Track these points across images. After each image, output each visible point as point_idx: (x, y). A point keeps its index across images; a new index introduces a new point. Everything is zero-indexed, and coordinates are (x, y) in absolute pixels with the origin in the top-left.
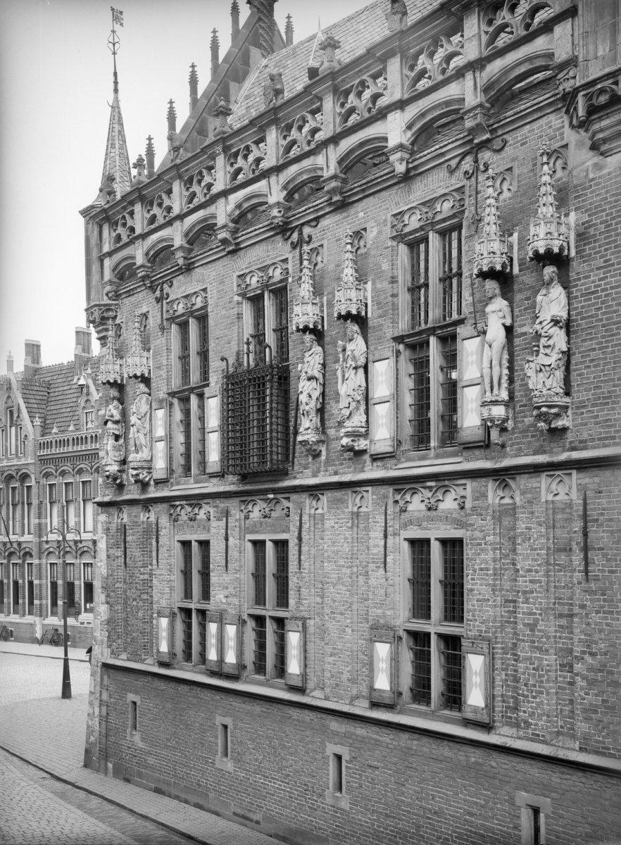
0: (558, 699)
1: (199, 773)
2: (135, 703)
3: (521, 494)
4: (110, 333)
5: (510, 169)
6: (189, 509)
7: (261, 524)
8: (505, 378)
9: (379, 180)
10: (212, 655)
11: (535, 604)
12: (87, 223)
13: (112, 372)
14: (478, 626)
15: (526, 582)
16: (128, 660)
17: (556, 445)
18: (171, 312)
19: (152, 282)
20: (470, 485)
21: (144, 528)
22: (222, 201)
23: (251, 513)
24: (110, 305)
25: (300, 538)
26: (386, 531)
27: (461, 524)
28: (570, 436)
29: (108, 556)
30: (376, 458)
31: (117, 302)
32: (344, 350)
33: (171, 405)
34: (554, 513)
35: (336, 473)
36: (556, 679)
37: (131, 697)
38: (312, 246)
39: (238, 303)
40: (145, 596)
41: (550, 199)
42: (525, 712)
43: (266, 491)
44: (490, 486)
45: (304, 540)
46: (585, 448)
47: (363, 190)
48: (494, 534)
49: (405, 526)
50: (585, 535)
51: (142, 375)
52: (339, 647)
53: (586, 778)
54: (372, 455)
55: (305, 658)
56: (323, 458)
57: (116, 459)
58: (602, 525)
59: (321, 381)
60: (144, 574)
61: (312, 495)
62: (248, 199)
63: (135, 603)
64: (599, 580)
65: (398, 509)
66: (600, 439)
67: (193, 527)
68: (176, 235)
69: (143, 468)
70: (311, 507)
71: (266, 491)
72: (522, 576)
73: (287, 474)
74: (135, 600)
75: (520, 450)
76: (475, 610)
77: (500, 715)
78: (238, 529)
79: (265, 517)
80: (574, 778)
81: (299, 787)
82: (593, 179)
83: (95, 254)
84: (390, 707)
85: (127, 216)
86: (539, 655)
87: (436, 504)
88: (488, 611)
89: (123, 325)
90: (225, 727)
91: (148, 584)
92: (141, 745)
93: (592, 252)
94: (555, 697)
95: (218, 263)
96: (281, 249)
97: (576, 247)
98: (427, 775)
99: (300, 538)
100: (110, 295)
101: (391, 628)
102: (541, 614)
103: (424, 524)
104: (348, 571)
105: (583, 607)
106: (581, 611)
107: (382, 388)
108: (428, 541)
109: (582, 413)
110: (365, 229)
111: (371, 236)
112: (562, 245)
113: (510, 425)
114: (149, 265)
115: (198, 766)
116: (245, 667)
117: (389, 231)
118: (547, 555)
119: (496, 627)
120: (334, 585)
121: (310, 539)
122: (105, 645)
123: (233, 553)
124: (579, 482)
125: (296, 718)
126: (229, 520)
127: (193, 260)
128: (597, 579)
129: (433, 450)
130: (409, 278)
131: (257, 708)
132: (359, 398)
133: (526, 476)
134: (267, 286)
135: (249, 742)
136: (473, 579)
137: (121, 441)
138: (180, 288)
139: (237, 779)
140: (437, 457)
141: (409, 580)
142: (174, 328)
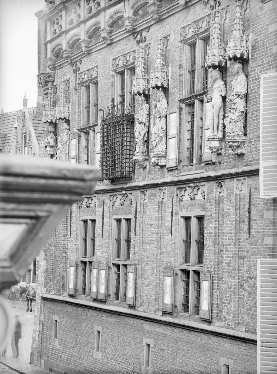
0: (239, 304)
1: (85, 362)
2: (56, 321)
4: (50, 91)
5: (228, 6)
6: (86, 200)
7: (120, 209)
8: (221, 125)
9: (174, 7)
10: (94, 289)
12: (39, 21)
13: (49, 115)
16: (55, 294)
18: (81, 79)
19: (71, 60)
22: (103, 13)
23: (115, 203)
24: (50, 73)
25: (136, 218)
26: (172, 212)
27: (204, 208)
28: (246, 158)
32: (156, 107)
33: (80, 136)
34: (240, 201)
35: (153, 179)
36: (238, 293)
37: (55, 317)
38: (146, 43)
39: (112, 76)
40: (64, 255)
41: (238, 27)
42: (225, 312)
43: (120, 190)
44: (214, 184)
45: (137, 218)
46: (251, 165)
47: (168, 12)
48: (215, 213)
49: (181, 209)
51: (65, 118)
52: (151, 281)
53: (247, 346)
54: (167, 168)
55: (136, 288)
56: (147, 169)
59: (147, 124)
60: (64, 241)
61: (142, 191)
62: (116, 13)
63: (59, 259)
65: (178, 200)
67: (88, 211)
68: (81, 33)
70: (141, 199)
71: (120, 190)
73: (131, 180)
74: (59, 257)
75: (227, 165)
77: (216, 315)
78: (108, 212)
79: (122, 205)
80: (242, 347)
81: (131, 365)
82: (259, 16)
83: (43, 42)
84: (171, 314)
85: (59, 18)
86: (231, 280)
87: (194, 196)
88: (212, 256)
89: (57, 86)
90: (99, 332)
91: (65, 246)
92: (58, 347)
93: (257, 56)
94: (237, 303)
95: (103, 50)
96: (130, 44)
97: (252, 53)
98: (185, 352)
99: (136, 218)
100: (50, 67)
101: (174, 268)
105: (248, 252)
107: (173, 131)
110: (169, 35)
111: (171, 39)
112: (242, 52)
113: (223, 151)
114: (70, 50)
115: (86, 358)
116: (110, 295)
117: (179, 37)
118: (235, 224)
119: (215, 265)
121: (140, 218)
122: (43, 286)
123: (106, 227)
125: (130, 324)
126: (105, 207)
127: (90, 48)
129: (194, 166)
130: (189, 64)
131: (113, 319)
132: (161, 135)
133: (228, 180)
134: (126, 66)
135: (109, 341)
138: (85, 65)
139: (103, 364)
140: (196, 169)
141: (183, 241)
142: (83, 89)
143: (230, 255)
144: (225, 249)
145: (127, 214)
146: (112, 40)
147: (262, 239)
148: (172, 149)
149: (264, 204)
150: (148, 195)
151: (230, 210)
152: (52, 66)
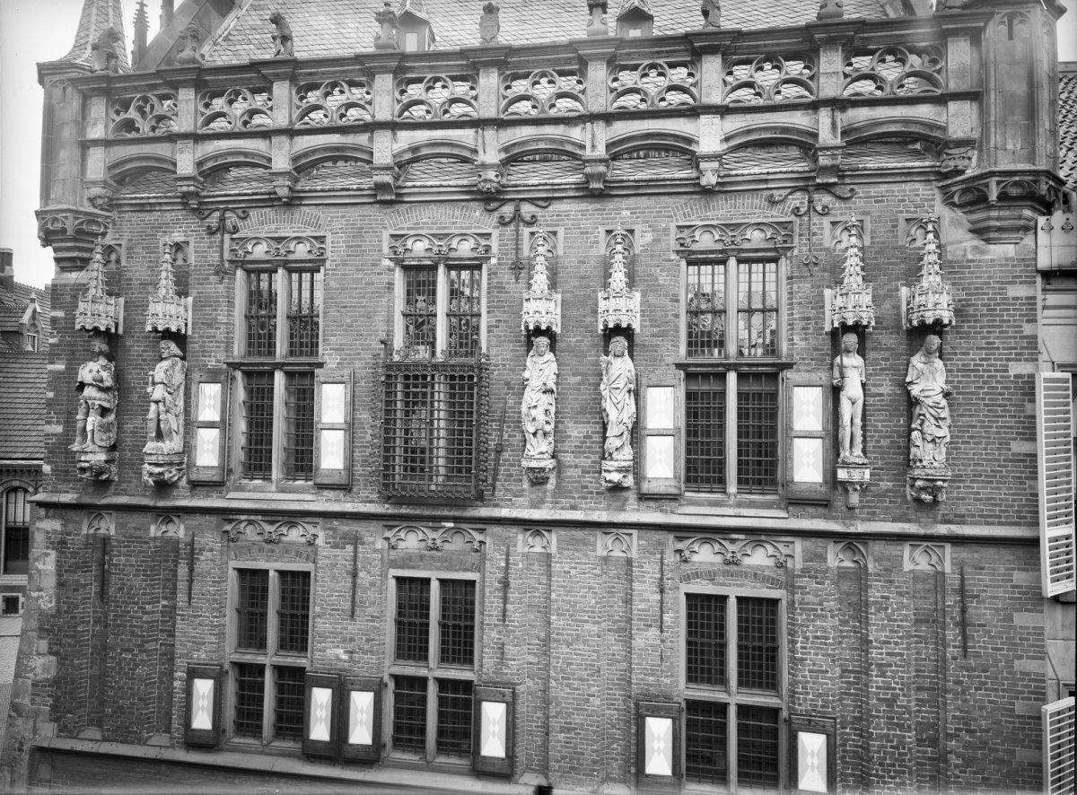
3: (875, 561)
7: (422, 557)
11: (893, 678)
14: (812, 700)
17: (924, 514)
19: (200, 204)
20: (799, 546)
21: (156, 547)
29: (61, 585)
30: (644, 498)
31: (109, 214)
33: (233, 378)
35: (574, 508)
39: (389, 270)
45: (512, 585)
46: (963, 523)
49: (687, 578)
50: (963, 611)
57: (103, 444)
58: (983, 602)
64: (980, 657)
66: (980, 516)
69: (171, 464)
70: (526, 543)
72: (876, 648)
76: (808, 682)
88: (827, 684)
100: (100, 201)
102: (902, 689)
104: (595, 628)
105: (958, 683)
106: (956, 687)
109: (959, 488)
114: (202, 179)
120: (569, 645)
124: (954, 555)
128: (977, 655)
136: (802, 648)
137: (111, 418)
144: (874, 673)
145: (456, 570)
146: (398, 195)
147: (1010, 666)
149: (1010, 599)
152: (106, 200)
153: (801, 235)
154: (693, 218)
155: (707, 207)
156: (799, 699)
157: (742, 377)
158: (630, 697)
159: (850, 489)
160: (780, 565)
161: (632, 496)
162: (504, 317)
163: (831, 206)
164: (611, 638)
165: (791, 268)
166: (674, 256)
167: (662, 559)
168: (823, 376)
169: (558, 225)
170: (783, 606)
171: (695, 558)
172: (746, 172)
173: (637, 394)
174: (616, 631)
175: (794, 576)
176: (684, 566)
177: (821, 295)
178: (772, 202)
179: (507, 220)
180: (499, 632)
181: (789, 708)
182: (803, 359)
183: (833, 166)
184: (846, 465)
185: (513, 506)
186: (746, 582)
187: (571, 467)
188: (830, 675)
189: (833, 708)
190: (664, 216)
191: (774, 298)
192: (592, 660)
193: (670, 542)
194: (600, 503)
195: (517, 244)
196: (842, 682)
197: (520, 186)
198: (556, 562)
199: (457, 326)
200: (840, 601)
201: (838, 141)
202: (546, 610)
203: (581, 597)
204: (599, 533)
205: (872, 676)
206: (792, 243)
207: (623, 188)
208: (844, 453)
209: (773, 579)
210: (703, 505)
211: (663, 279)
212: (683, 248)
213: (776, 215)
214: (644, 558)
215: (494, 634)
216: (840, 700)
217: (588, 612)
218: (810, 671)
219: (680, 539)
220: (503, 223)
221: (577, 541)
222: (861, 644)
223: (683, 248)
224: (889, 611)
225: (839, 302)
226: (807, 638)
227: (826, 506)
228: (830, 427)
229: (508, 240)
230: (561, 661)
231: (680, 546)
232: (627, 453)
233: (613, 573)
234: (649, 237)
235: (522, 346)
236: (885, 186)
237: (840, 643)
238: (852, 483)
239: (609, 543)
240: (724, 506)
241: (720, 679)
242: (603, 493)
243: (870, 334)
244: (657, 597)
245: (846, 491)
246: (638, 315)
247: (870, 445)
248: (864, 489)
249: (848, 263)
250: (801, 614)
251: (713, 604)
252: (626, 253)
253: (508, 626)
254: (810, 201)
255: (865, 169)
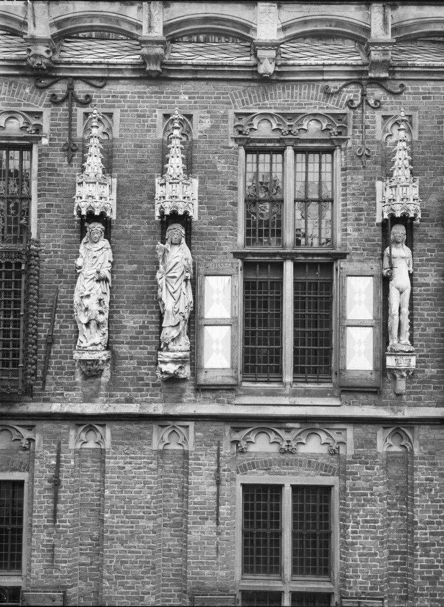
3: (421, 444)
14: (361, 583)
15: (426, 534)
20: (350, 433)
30: (201, 389)
35: (129, 401)
45: (63, 484)
49: (243, 469)
70: (78, 439)
72: (421, 528)
76: (357, 566)
88: (375, 566)
103: (276, 468)
104: (151, 524)
108: (279, 488)
120: (123, 542)
133: (428, 426)
136: (353, 532)
143: (436, 564)
144: (419, 553)
148: (214, 346)
150: (112, 435)
151: (435, 482)
153: (354, 127)
154: (251, 105)
155: (265, 95)
156: (350, 582)
157: (298, 267)
158: (185, 592)
159: (398, 376)
160: (334, 453)
161: (189, 388)
162: (57, 201)
163: (382, 100)
164: (167, 533)
165: (346, 159)
166: (232, 144)
167: (219, 450)
168: (374, 266)
169: (113, 107)
170: (336, 492)
171: (252, 448)
172: (303, 62)
173: (194, 283)
174: (171, 526)
175: (346, 463)
176: (240, 457)
177: (373, 187)
178: (328, 94)
179: (60, 98)
180: (49, 534)
181: (341, 592)
182: (356, 249)
183: (384, 61)
184: (395, 353)
185: (64, 400)
186: (301, 469)
187: (126, 358)
188: (378, 557)
189: (381, 589)
190: (223, 103)
191: (330, 189)
192: (147, 557)
193: (227, 433)
194: (156, 395)
195: (70, 125)
196: (390, 564)
197: (72, 63)
198: (110, 458)
199: (5, 209)
200: (388, 484)
201: (389, 38)
202: (99, 510)
203: (136, 492)
204: (155, 427)
205: (417, 555)
206: (346, 135)
207: (182, 71)
208: (393, 342)
209: (326, 466)
210: (260, 395)
211: (221, 166)
212: (240, 136)
213: (332, 106)
214: (201, 450)
215: (44, 536)
216: (388, 581)
217: (143, 507)
218: (360, 555)
219: (237, 430)
220: (55, 101)
221: (133, 435)
222: (408, 526)
223: (240, 136)
224: (433, 492)
225: (389, 194)
226: (358, 523)
227: (375, 393)
228: (380, 316)
229: (60, 119)
230: (115, 560)
231: (237, 436)
232: (184, 343)
233: (169, 467)
234: (207, 123)
235: (75, 232)
236: (432, 83)
237: (388, 525)
238: (399, 370)
239: (166, 437)
240: (280, 395)
241: (275, 567)
242: (159, 385)
243: (418, 226)
244: (214, 489)
245: (395, 378)
246: (196, 203)
247: (417, 333)
248: (411, 375)
249: (397, 156)
250: (352, 500)
251: (269, 493)
252: (184, 139)
253: (59, 526)
254: (363, 95)
255: (414, 66)
